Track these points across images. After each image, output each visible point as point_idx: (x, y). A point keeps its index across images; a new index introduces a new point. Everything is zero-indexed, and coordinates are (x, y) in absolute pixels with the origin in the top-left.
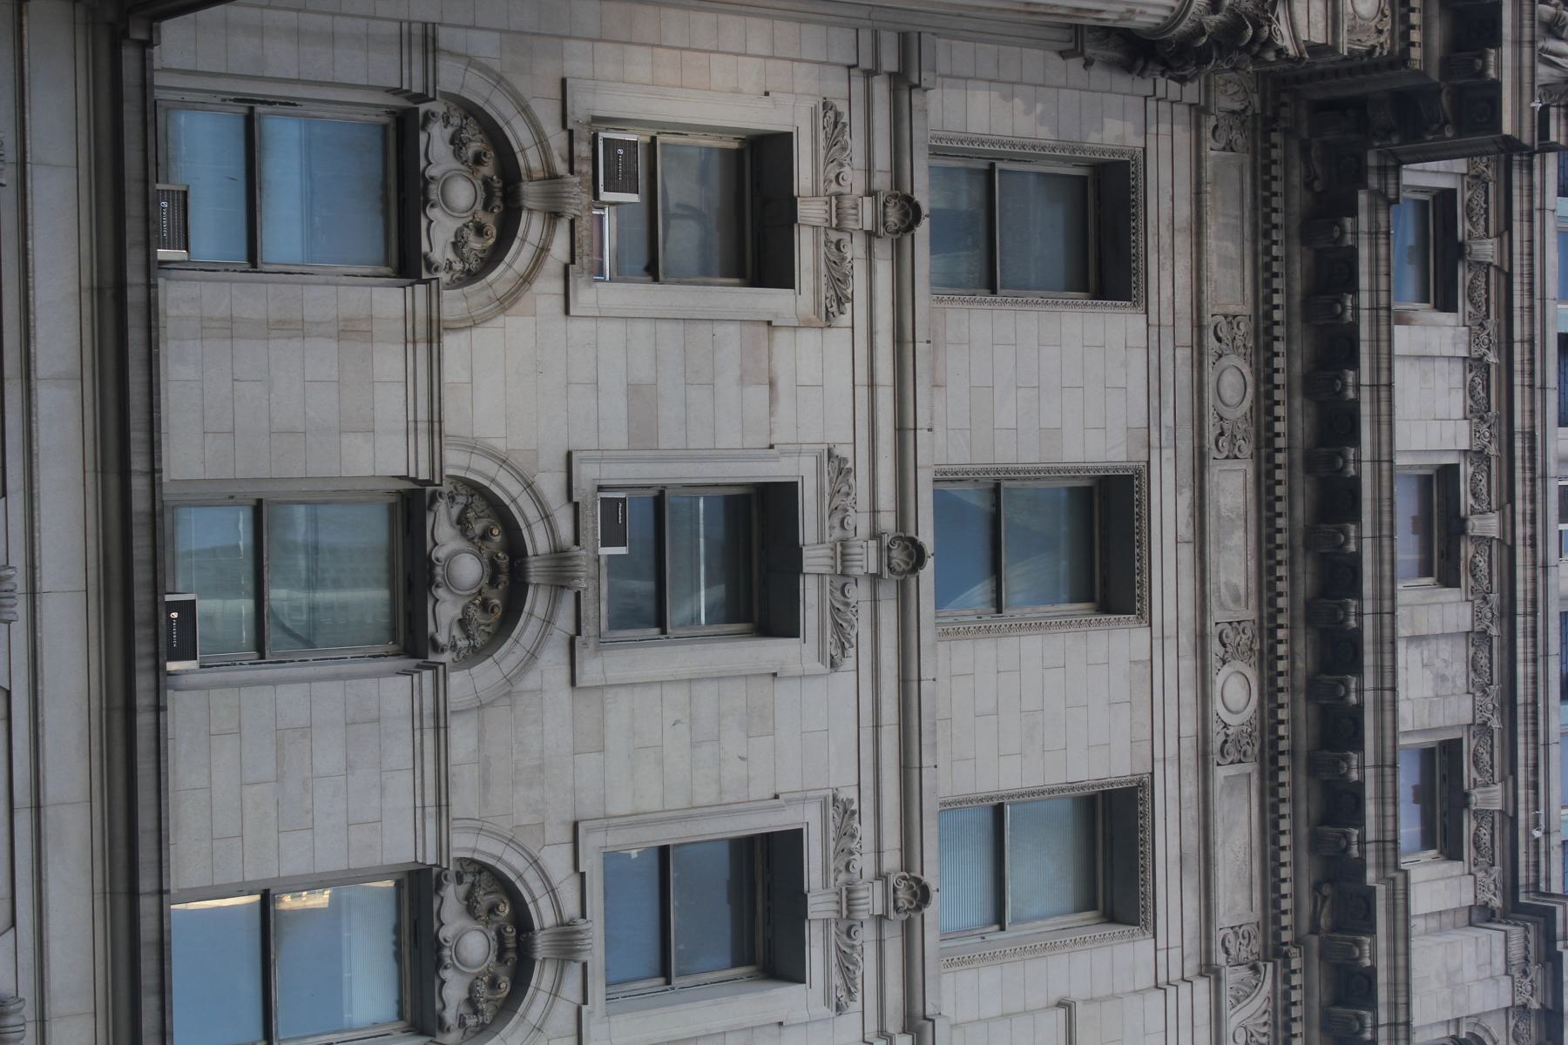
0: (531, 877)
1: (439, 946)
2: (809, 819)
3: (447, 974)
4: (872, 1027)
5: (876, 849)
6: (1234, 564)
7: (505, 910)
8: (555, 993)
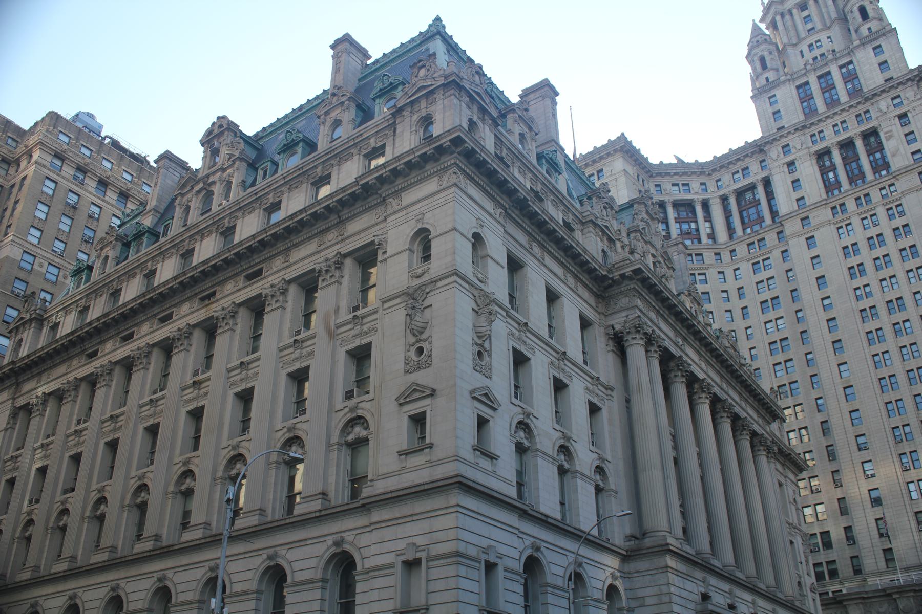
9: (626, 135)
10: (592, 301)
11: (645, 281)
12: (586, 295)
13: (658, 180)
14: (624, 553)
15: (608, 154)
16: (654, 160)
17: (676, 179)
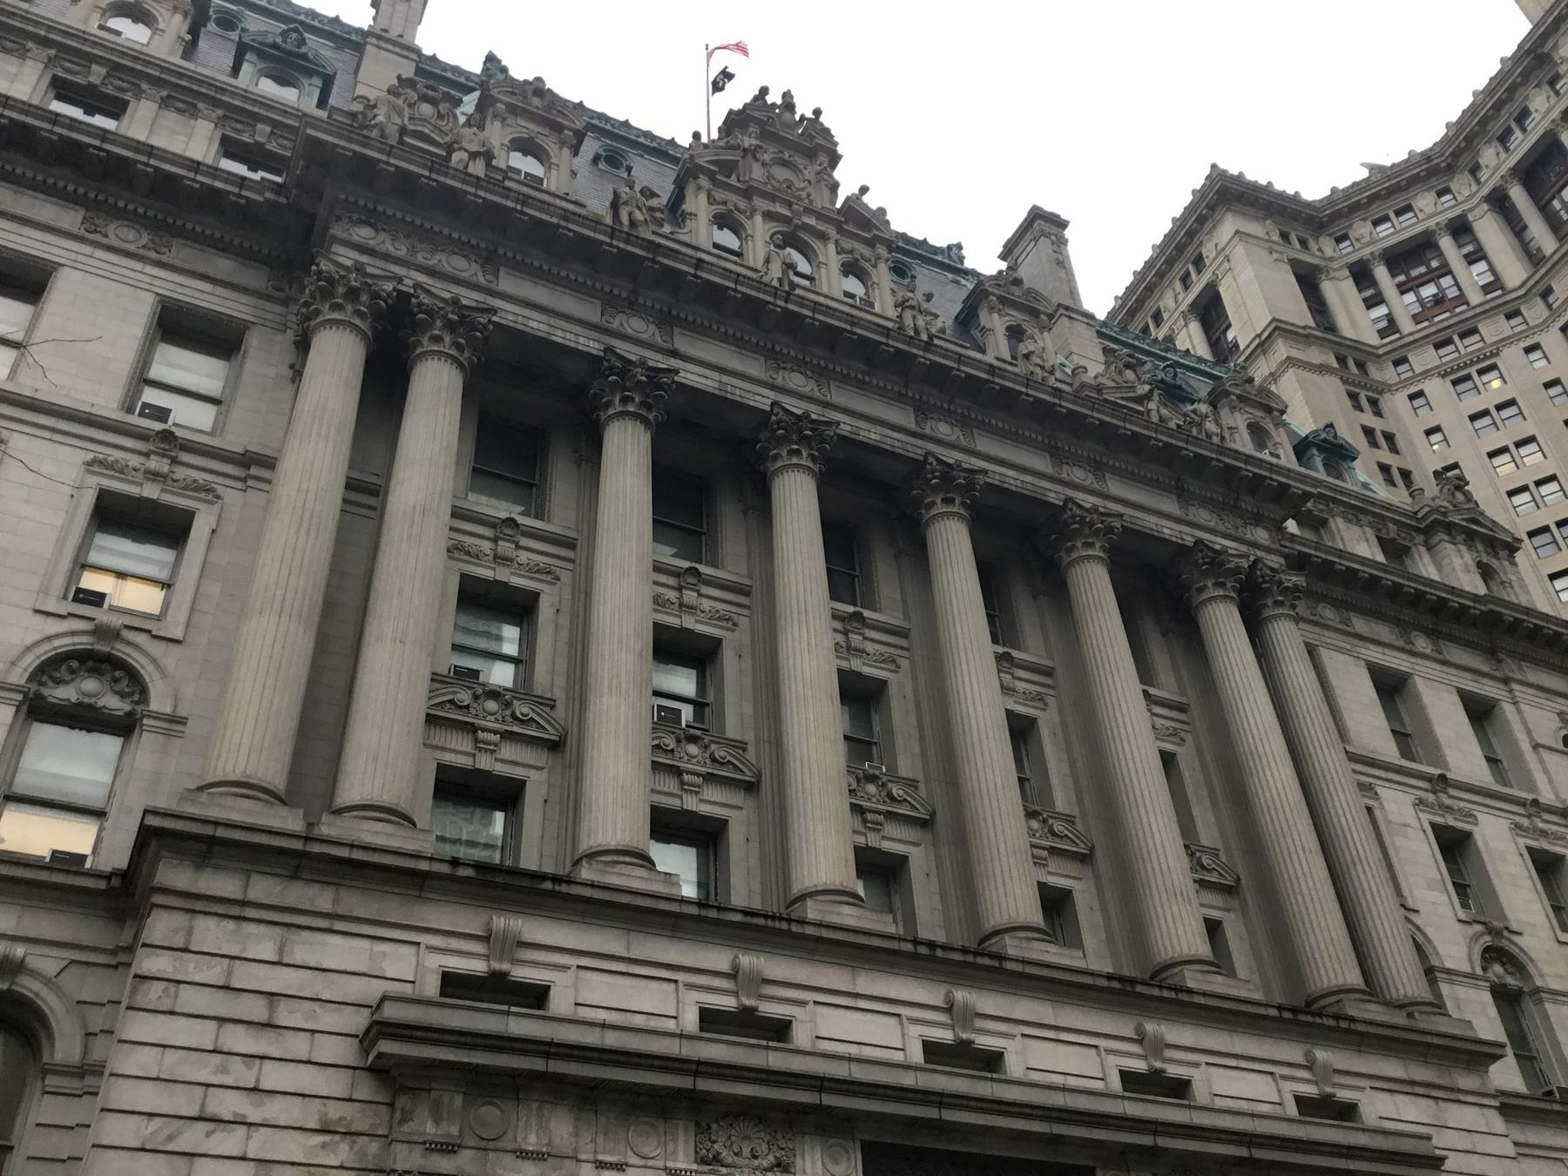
0: (56, 643)
1: (79, 705)
2: (95, 482)
3: (101, 703)
4: (239, 485)
5: (125, 453)
6: (45, 210)
7: (75, 664)
8: (136, 647)
9: (1222, 166)
10: (255, 278)
11: (364, 171)
12: (223, 265)
13: (1338, 229)
14: (102, 885)
15: (1201, 220)
16: (1313, 189)
17: (1377, 210)
